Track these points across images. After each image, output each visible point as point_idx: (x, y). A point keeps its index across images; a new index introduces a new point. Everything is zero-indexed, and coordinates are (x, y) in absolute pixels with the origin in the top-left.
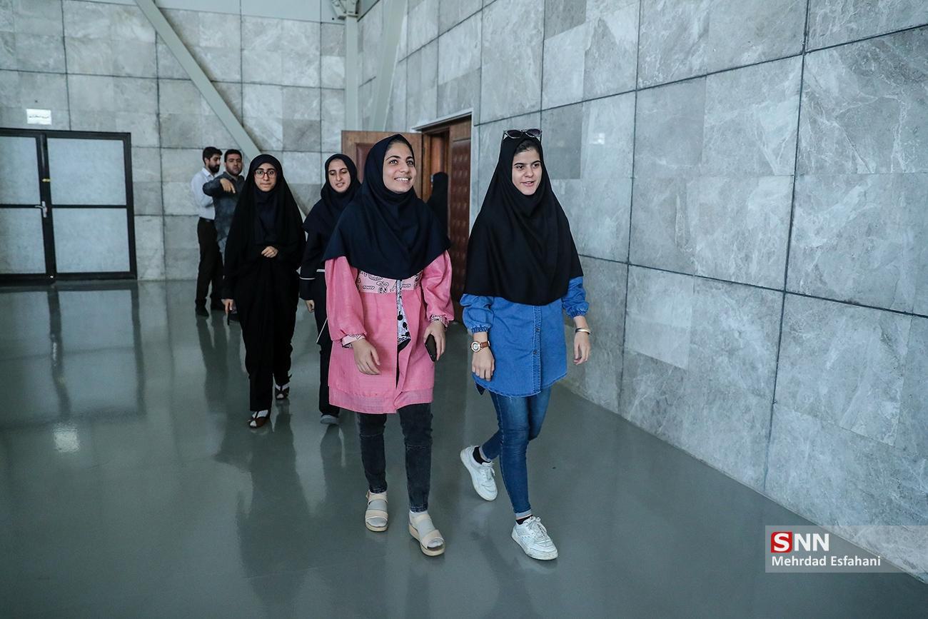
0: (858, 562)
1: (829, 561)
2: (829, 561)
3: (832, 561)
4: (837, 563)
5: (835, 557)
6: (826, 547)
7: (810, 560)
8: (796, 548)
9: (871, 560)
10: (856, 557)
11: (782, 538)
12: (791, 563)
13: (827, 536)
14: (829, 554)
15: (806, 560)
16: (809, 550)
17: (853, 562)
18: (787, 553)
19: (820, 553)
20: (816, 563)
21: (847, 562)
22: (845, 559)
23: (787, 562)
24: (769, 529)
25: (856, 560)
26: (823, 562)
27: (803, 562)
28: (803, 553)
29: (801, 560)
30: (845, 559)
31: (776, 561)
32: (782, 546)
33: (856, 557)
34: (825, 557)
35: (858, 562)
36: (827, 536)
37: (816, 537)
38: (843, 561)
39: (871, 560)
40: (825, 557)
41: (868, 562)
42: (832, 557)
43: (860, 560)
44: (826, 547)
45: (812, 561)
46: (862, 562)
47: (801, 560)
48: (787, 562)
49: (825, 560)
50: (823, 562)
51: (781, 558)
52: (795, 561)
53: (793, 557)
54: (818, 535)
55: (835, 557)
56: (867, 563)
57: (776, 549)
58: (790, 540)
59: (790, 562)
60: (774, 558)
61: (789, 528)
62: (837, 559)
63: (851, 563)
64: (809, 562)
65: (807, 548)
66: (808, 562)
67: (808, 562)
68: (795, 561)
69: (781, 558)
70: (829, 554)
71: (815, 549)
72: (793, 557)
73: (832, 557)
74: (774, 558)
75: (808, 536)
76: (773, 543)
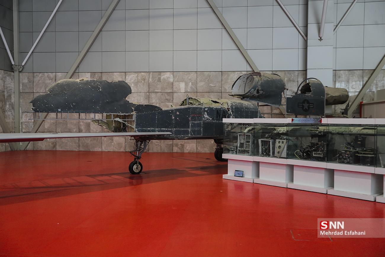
0: (356, 233)
1: (344, 233)
2: (344, 233)
3: (345, 233)
4: (347, 234)
5: (347, 231)
6: (343, 227)
7: (336, 232)
8: (330, 228)
9: (362, 233)
10: (355, 231)
11: (324, 223)
12: (328, 234)
13: (343, 223)
14: (344, 230)
15: (335, 232)
16: (336, 228)
17: (354, 233)
18: (326, 230)
19: (340, 230)
20: (339, 234)
21: (352, 233)
22: (351, 232)
23: (327, 233)
24: (319, 220)
25: (355, 233)
26: (341, 233)
27: (333, 233)
28: (333, 230)
29: (332, 233)
30: (351, 232)
31: (322, 233)
32: (324, 227)
33: (355, 231)
34: (342, 231)
35: (356, 233)
36: (343, 223)
37: (339, 223)
38: (350, 233)
39: (362, 233)
40: (342, 231)
41: (360, 233)
42: (345, 231)
43: (357, 233)
44: (343, 227)
45: (337, 233)
46: (358, 233)
47: (332, 233)
48: (327, 233)
49: (342, 232)
50: (341, 233)
51: (324, 232)
52: (330, 233)
53: (329, 231)
54: (339, 222)
55: (347, 231)
56: (360, 234)
57: (322, 228)
58: (328, 224)
59: (328, 233)
60: (321, 232)
61: (328, 219)
62: (347, 232)
63: (353, 234)
64: (336, 233)
65: (335, 227)
66: (335, 233)
67: (335, 233)
68: (330, 233)
69: (324, 232)
70: (344, 230)
71: (338, 228)
72: (329, 231)
73: (345, 231)
74: (321, 232)
75: (335, 222)
76: (321, 226)
